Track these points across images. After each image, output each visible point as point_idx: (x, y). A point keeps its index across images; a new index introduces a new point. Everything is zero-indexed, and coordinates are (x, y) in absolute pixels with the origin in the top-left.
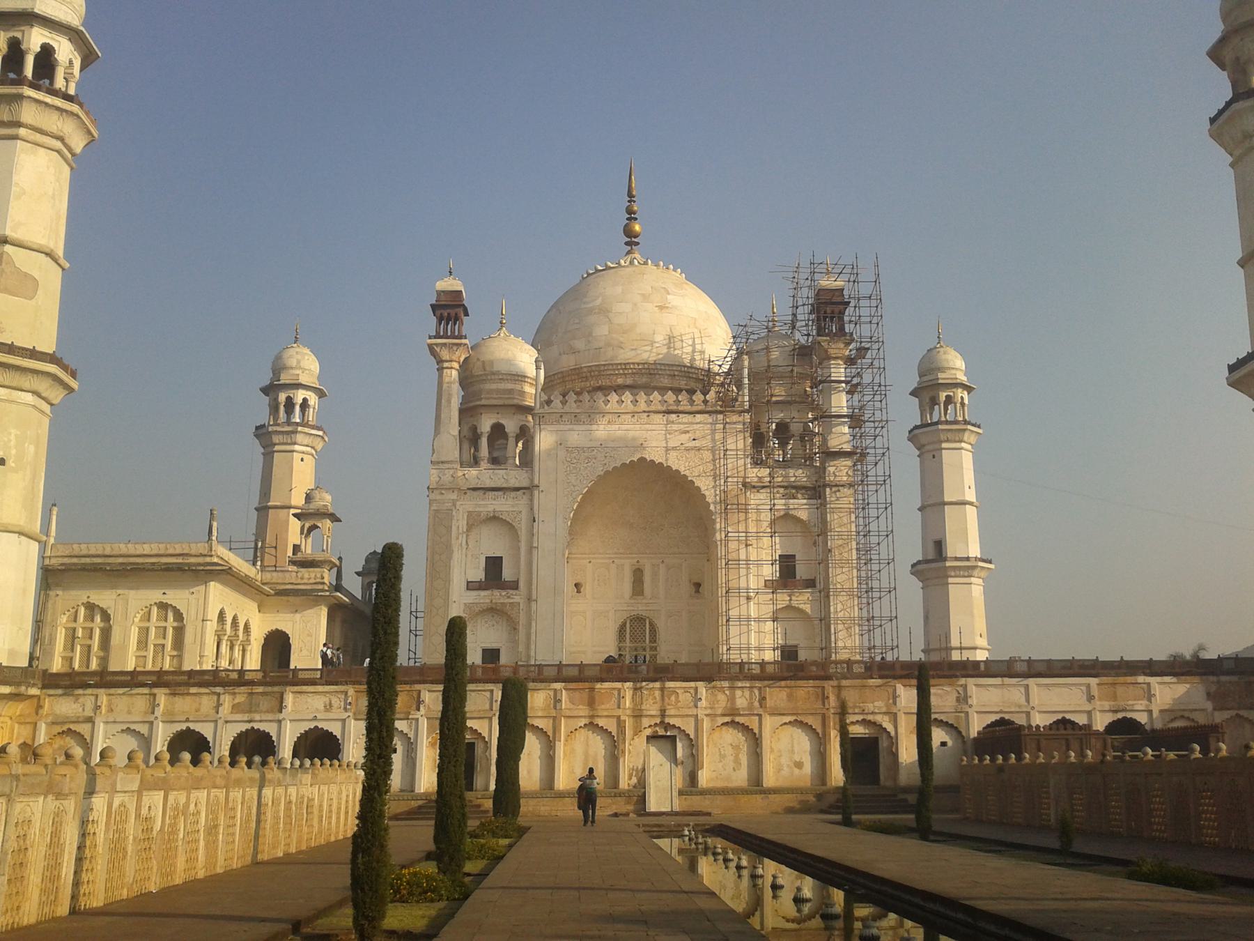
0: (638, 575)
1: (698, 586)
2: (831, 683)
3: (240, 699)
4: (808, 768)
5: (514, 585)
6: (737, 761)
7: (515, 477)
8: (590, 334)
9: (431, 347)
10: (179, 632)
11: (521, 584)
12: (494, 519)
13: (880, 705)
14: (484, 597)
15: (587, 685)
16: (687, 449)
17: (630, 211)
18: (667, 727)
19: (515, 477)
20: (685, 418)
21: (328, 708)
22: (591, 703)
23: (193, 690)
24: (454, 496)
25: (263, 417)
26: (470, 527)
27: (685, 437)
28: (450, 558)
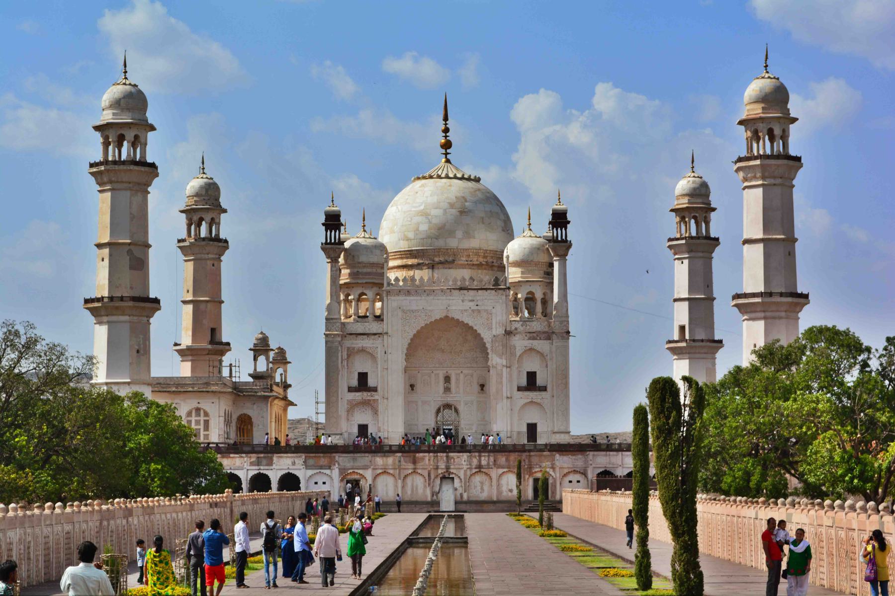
0: (447, 379)
1: (482, 386)
2: (524, 455)
3: (253, 459)
4: (515, 492)
5: (375, 389)
6: (482, 489)
7: (374, 327)
8: (417, 230)
9: (323, 249)
10: (207, 423)
11: (379, 389)
12: (363, 350)
13: (546, 464)
14: (358, 396)
15: (412, 454)
16: (473, 311)
17: (446, 130)
18: (450, 473)
19: (374, 327)
20: (472, 293)
21: (294, 464)
22: (414, 462)
23: (232, 455)
24: (339, 339)
25: (183, 234)
26: (349, 356)
27: (471, 304)
28: (338, 374)
